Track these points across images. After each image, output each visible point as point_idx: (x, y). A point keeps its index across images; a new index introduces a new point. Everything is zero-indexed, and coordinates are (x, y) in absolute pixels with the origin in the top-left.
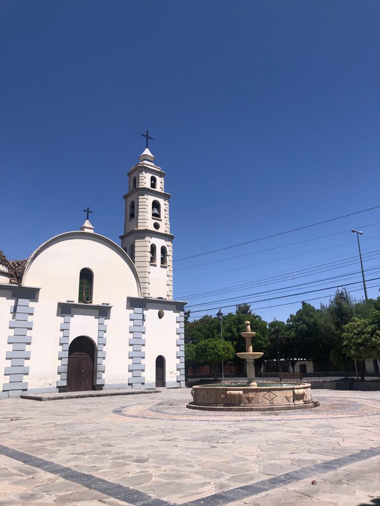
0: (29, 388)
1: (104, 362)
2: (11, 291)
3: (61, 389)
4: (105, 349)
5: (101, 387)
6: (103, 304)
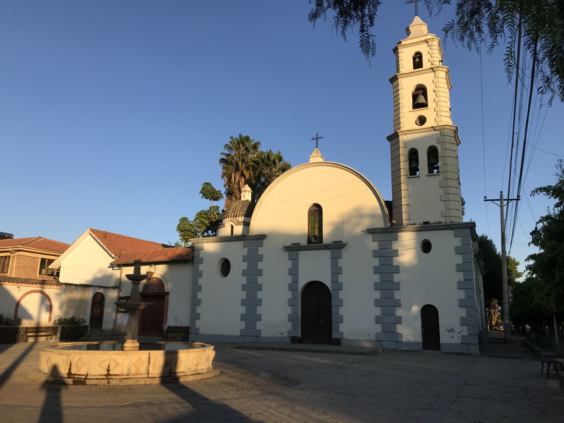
0: (263, 335)
1: (342, 311)
2: (242, 243)
3: (294, 340)
4: (341, 295)
5: (338, 342)
6: (334, 242)
